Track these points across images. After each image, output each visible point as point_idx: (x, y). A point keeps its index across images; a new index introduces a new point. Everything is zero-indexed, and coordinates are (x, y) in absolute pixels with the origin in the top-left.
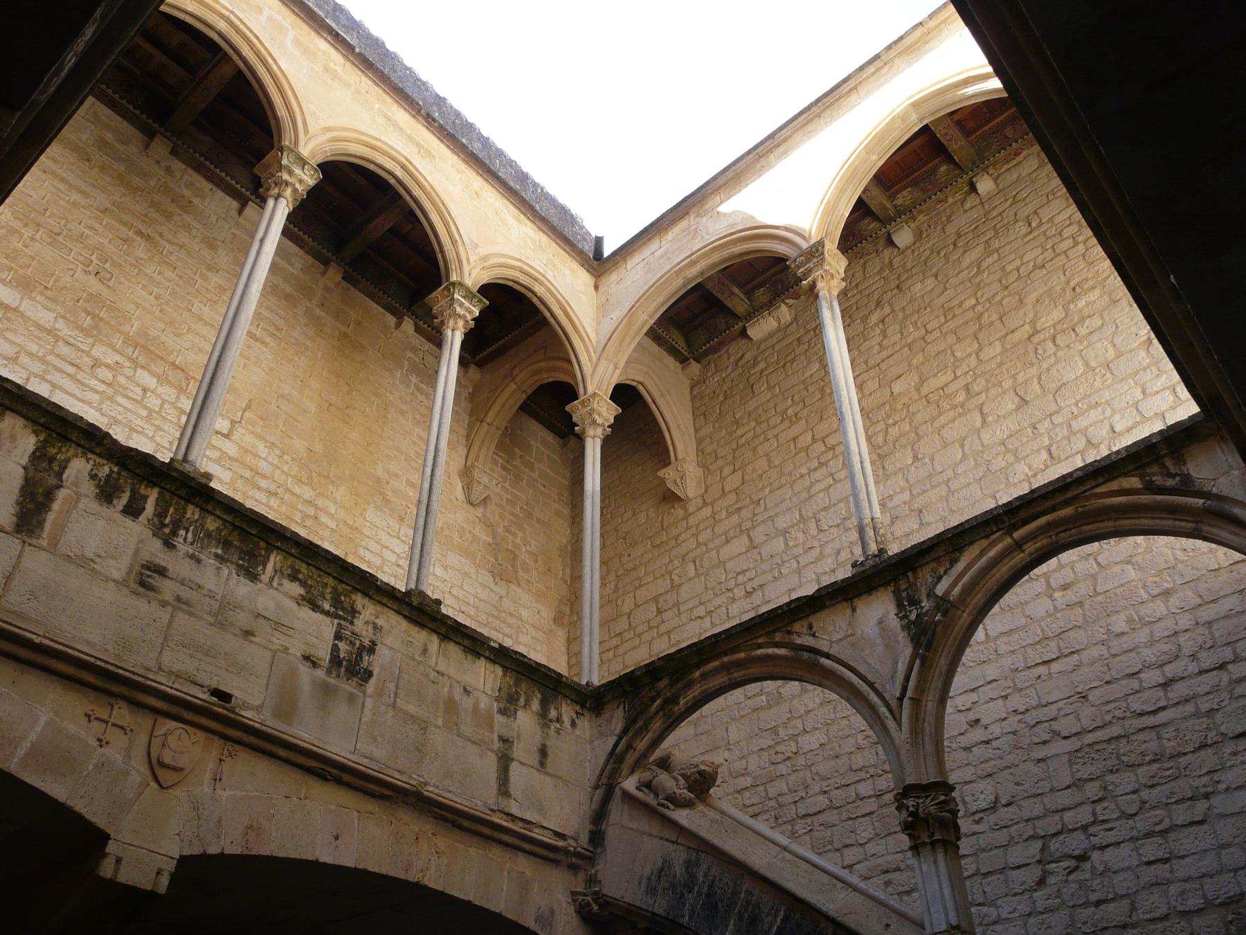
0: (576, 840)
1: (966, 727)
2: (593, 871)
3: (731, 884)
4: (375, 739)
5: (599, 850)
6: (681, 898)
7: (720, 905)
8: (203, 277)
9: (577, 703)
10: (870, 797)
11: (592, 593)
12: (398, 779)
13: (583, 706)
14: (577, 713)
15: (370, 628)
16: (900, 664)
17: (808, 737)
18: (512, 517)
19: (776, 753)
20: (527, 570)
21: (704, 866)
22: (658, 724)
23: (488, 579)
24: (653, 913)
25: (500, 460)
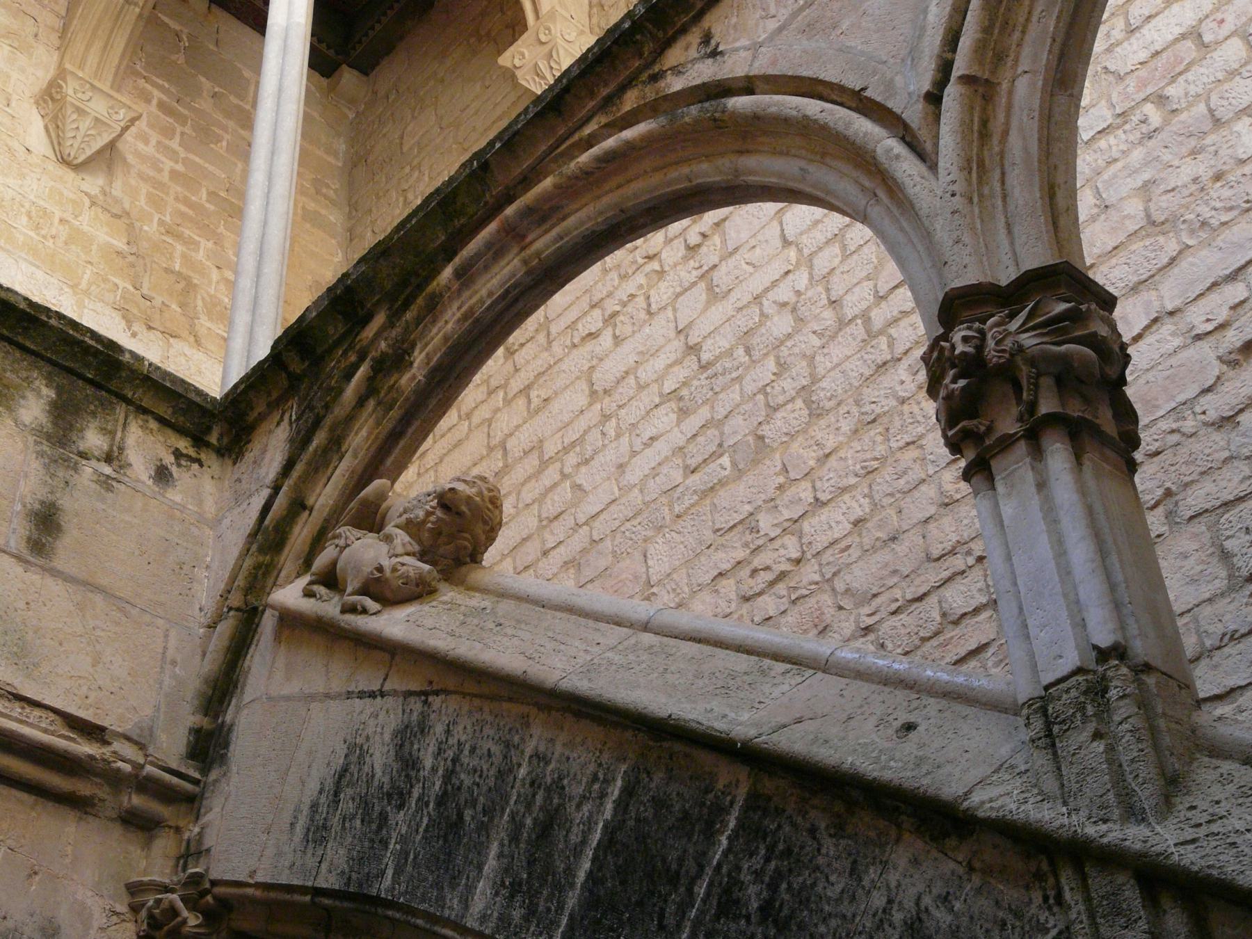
0: (142, 747)
1: (1216, 369)
2: (197, 830)
3: (496, 750)
5: (213, 775)
6: (380, 828)
7: (468, 814)
9: (180, 431)
10: (976, 611)
11: (265, 224)
13: (199, 441)
14: (178, 454)
16: (931, 18)
17: (825, 514)
18: (183, 208)
19: (755, 572)
21: (439, 729)
22: (364, 433)
24: (317, 892)
25: (156, 93)
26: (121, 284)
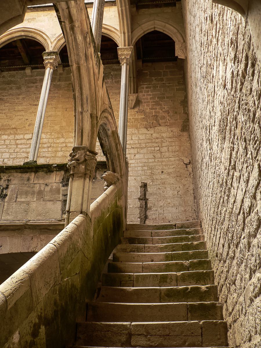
4: (9, 214)
8: (18, 99)
12: (18, 223)
15: (6, 182)
20: (163, 118)
23: (144, 131)
26: (145, 123)
